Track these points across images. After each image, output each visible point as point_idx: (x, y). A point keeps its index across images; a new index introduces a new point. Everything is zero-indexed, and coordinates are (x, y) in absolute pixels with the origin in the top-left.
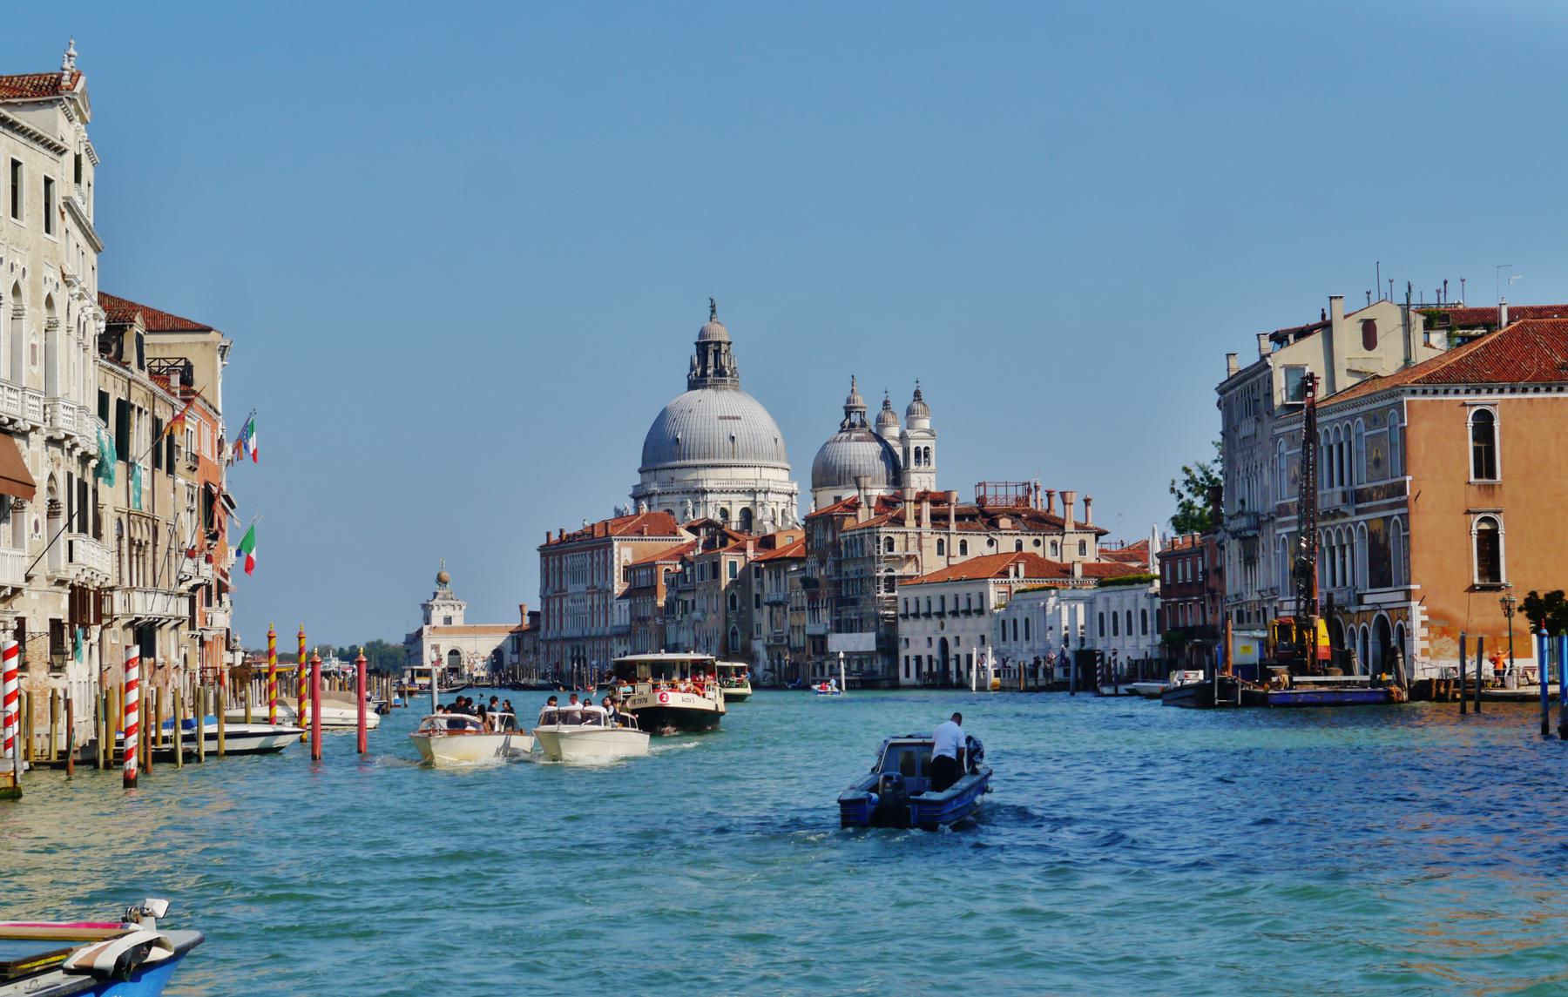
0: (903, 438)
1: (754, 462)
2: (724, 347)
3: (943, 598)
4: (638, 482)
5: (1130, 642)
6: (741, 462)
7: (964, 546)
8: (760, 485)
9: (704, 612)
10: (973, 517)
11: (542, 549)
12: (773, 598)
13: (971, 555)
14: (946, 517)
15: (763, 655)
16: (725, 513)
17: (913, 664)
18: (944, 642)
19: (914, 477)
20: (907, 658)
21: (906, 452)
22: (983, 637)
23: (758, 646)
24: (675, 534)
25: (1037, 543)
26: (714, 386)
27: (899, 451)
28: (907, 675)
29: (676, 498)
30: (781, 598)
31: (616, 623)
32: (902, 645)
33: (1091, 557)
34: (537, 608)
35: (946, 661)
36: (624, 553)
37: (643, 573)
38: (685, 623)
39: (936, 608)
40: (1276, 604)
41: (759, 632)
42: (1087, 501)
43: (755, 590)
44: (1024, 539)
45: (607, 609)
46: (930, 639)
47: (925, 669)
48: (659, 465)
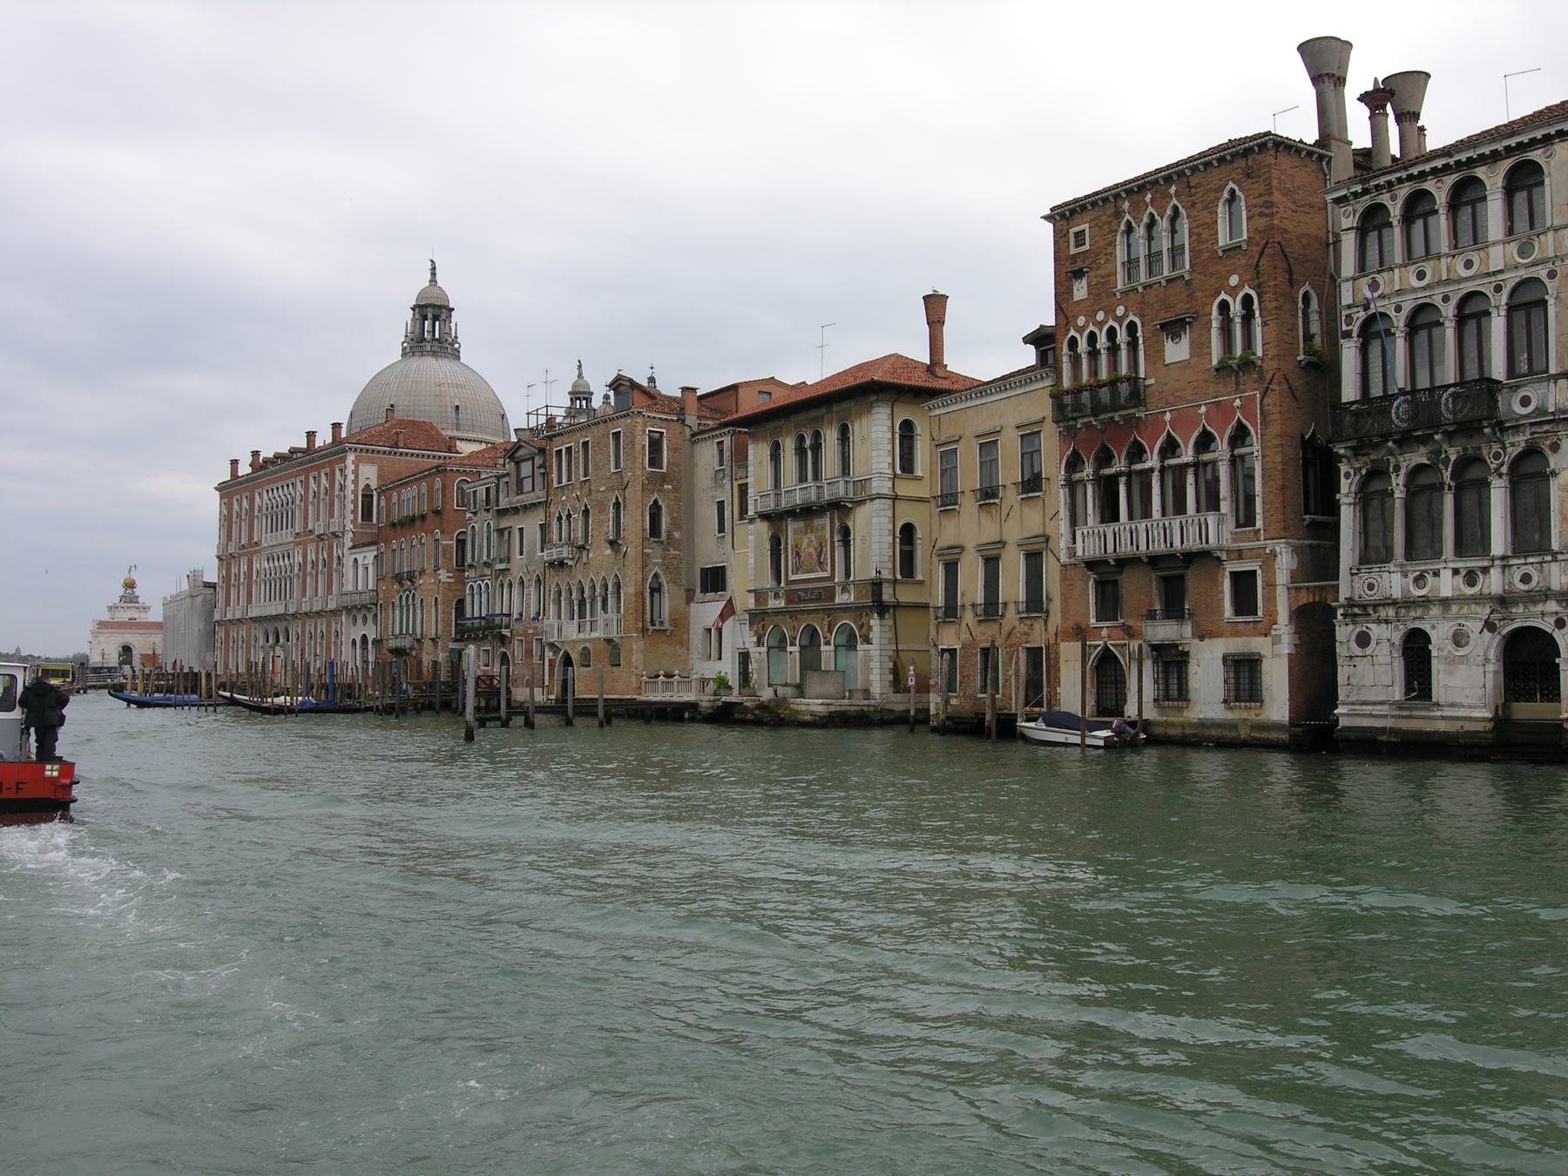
11: (222, 488)
26: (434, 354)
31: (349, 587)
45: (331, 567)
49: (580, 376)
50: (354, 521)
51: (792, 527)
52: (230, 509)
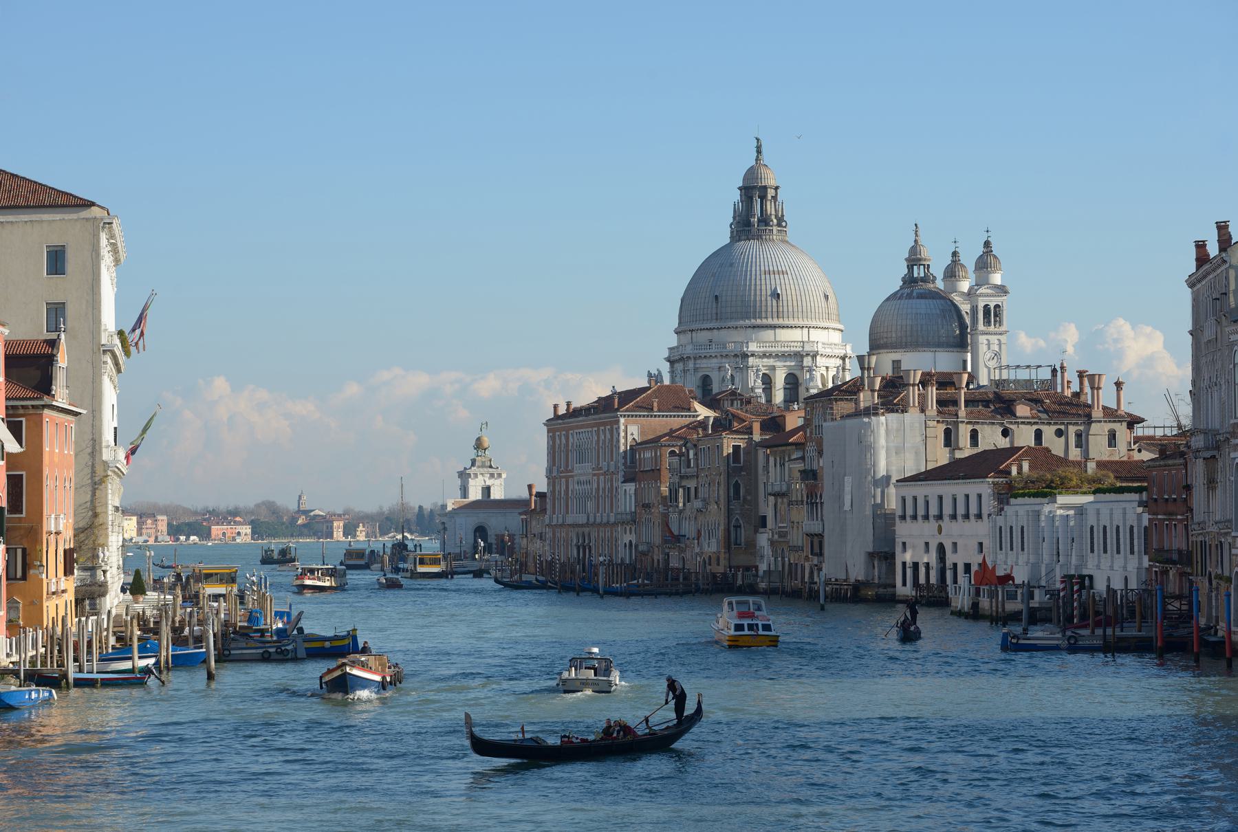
0: (970, 294)
1: (801, 323)
2: (771, 193)
3: (941, 498)
4: (675, 344)
5: (1119, 561)
6: (786, 322)
7: (974, 435)
8: (807, 348)
9: (704, 500)
10: (986, 403)
12: (777, 489)
13: (982, 447)
14: (955, 403)
15: (767, 551)
16: (768, 381)
17: (909, 572)
18: (941, 549)
19: (982, 339)
20: (904, 564)
21: (974, 310)
22: (981, 544)
23: (763, 540)
24: (689, 410)
25: (1059, 433)
26: (759, 237)
27: (965, 308)
28: (904, 584)
29: (714, 362)
30: (784, 488)
32: (898, 549)
33: (1121, 452)
34: (542, 486)
35: (942, 572)
36: (630, 430)
37: (648, 455)
38: (688, 513)
39: (933, 511)
40: (1230, 540)
41: (764, 525)
42: (1119, 385)
43: (762, 478)
44: (1044, 428)
45: (612, 494)
46: (927, 544)
47: (922, 580)
48: (693, 327)
49: (916, 241)
50: (624, 464)
51: (779, 500)
52: (554, 442)
